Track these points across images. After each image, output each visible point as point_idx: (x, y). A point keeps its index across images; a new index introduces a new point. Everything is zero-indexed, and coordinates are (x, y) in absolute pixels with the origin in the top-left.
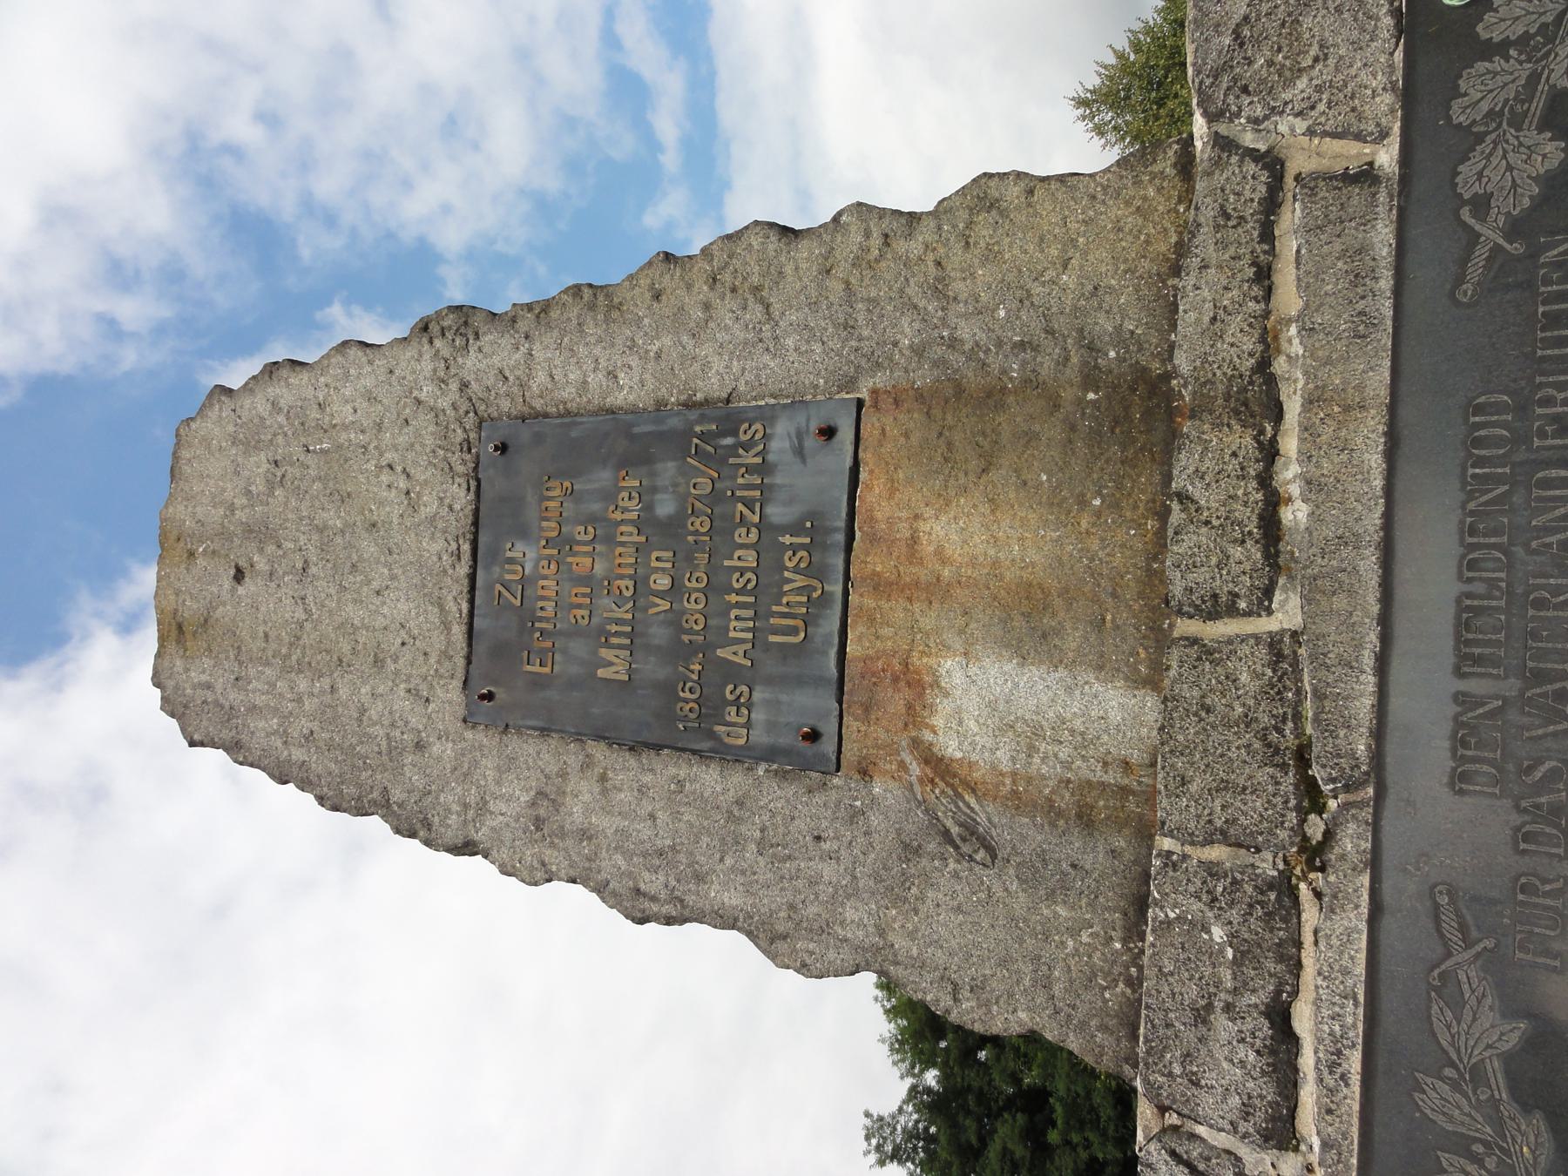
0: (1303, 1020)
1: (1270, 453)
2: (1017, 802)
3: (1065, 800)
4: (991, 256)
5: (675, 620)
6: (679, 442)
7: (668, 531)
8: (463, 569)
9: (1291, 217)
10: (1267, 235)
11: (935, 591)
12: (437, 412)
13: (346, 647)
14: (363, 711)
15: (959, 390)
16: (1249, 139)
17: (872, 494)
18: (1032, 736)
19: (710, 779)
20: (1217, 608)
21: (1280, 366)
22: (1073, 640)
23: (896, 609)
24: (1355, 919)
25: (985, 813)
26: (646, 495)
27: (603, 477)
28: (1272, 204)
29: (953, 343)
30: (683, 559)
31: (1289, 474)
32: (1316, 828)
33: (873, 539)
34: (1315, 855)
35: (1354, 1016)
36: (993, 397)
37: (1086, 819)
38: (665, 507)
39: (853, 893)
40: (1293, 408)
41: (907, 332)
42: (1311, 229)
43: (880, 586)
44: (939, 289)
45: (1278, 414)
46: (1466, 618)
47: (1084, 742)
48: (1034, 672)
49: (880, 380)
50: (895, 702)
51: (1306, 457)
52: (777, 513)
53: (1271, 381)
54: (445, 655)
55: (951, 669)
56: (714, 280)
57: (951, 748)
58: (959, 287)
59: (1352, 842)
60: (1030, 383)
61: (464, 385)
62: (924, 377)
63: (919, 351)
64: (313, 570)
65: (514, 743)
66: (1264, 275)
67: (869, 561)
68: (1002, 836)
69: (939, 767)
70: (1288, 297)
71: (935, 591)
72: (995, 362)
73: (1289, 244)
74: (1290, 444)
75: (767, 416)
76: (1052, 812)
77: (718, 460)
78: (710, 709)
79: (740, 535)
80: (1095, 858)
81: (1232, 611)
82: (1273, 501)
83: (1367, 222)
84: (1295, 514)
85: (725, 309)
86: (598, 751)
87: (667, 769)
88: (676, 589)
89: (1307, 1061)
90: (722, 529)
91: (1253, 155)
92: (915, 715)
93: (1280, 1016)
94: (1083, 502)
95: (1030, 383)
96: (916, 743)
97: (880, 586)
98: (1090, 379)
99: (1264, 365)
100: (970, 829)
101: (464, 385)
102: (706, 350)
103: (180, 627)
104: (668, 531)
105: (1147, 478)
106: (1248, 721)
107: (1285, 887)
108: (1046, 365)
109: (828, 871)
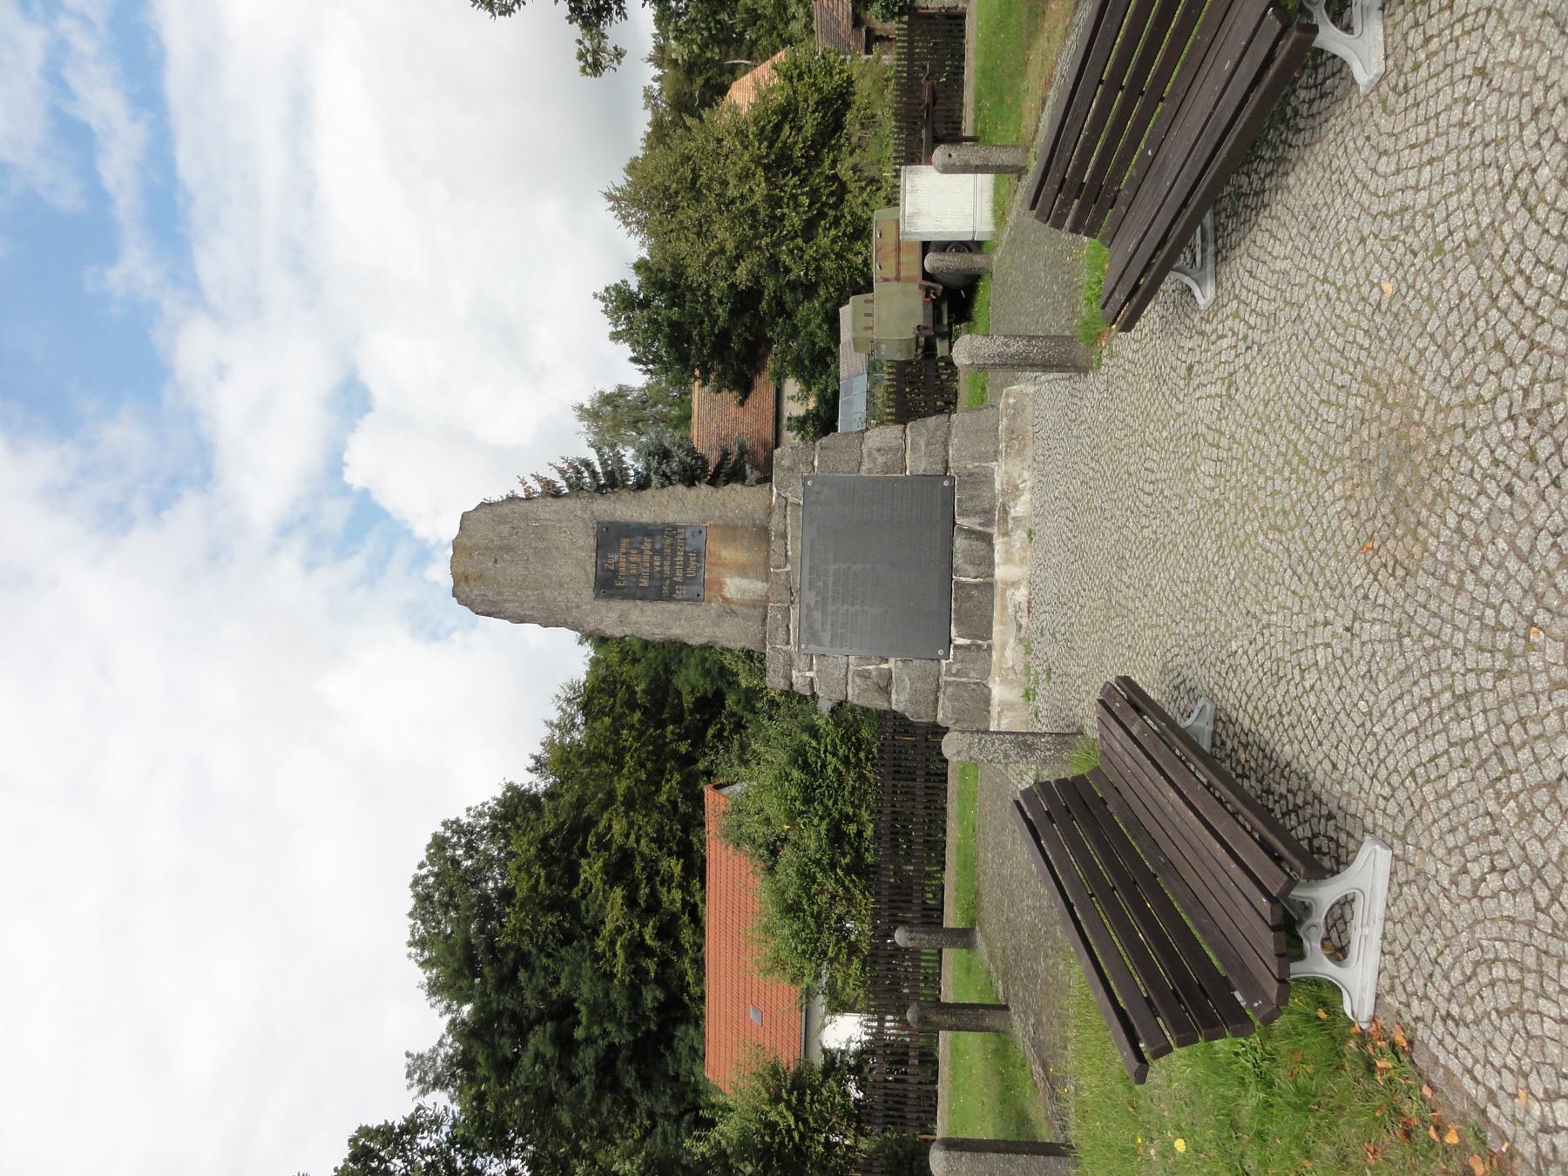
2: (741, 605)
5: (661, 572)
7: (660, 552)
8: (594, 560)
9: (789, 508)
11: (724, 565)
12: (583, 519)
18: (744, 592)
19: (672, 606)
20: (778, 567)
25: (735, 607)
26: (653, 543)
27: (639, 538)
30: (663, 558)
36: (735, 528)
37: (754, 606)
38: (658, 546)
41: (717, 513)
43: (713, 564)
44: (724, 505)
46: (811, 568)
47: (754, 593)
50: (716, 587)
52: (688, 549)
54: (587, 582)
55: (728, 580)
57: (728, 596)
59: (797, 600)
62: (721, 523)
63: (720, 517)
67: (709, 559)
68: (739, 612)
69: (726, 600)
70: (789, 521)
71: (724, 565)
75: (685, 527)
76: (748, 606)
77: (673, 536)
78: (672, 591)
80: (756, 613)
84: (790, 553)
86: (639, 603)
88: (661, 565)
90: (674, 553)
92: (720, 590)
97: (713, 564)
100: (732, 611)
109: (702, 623)
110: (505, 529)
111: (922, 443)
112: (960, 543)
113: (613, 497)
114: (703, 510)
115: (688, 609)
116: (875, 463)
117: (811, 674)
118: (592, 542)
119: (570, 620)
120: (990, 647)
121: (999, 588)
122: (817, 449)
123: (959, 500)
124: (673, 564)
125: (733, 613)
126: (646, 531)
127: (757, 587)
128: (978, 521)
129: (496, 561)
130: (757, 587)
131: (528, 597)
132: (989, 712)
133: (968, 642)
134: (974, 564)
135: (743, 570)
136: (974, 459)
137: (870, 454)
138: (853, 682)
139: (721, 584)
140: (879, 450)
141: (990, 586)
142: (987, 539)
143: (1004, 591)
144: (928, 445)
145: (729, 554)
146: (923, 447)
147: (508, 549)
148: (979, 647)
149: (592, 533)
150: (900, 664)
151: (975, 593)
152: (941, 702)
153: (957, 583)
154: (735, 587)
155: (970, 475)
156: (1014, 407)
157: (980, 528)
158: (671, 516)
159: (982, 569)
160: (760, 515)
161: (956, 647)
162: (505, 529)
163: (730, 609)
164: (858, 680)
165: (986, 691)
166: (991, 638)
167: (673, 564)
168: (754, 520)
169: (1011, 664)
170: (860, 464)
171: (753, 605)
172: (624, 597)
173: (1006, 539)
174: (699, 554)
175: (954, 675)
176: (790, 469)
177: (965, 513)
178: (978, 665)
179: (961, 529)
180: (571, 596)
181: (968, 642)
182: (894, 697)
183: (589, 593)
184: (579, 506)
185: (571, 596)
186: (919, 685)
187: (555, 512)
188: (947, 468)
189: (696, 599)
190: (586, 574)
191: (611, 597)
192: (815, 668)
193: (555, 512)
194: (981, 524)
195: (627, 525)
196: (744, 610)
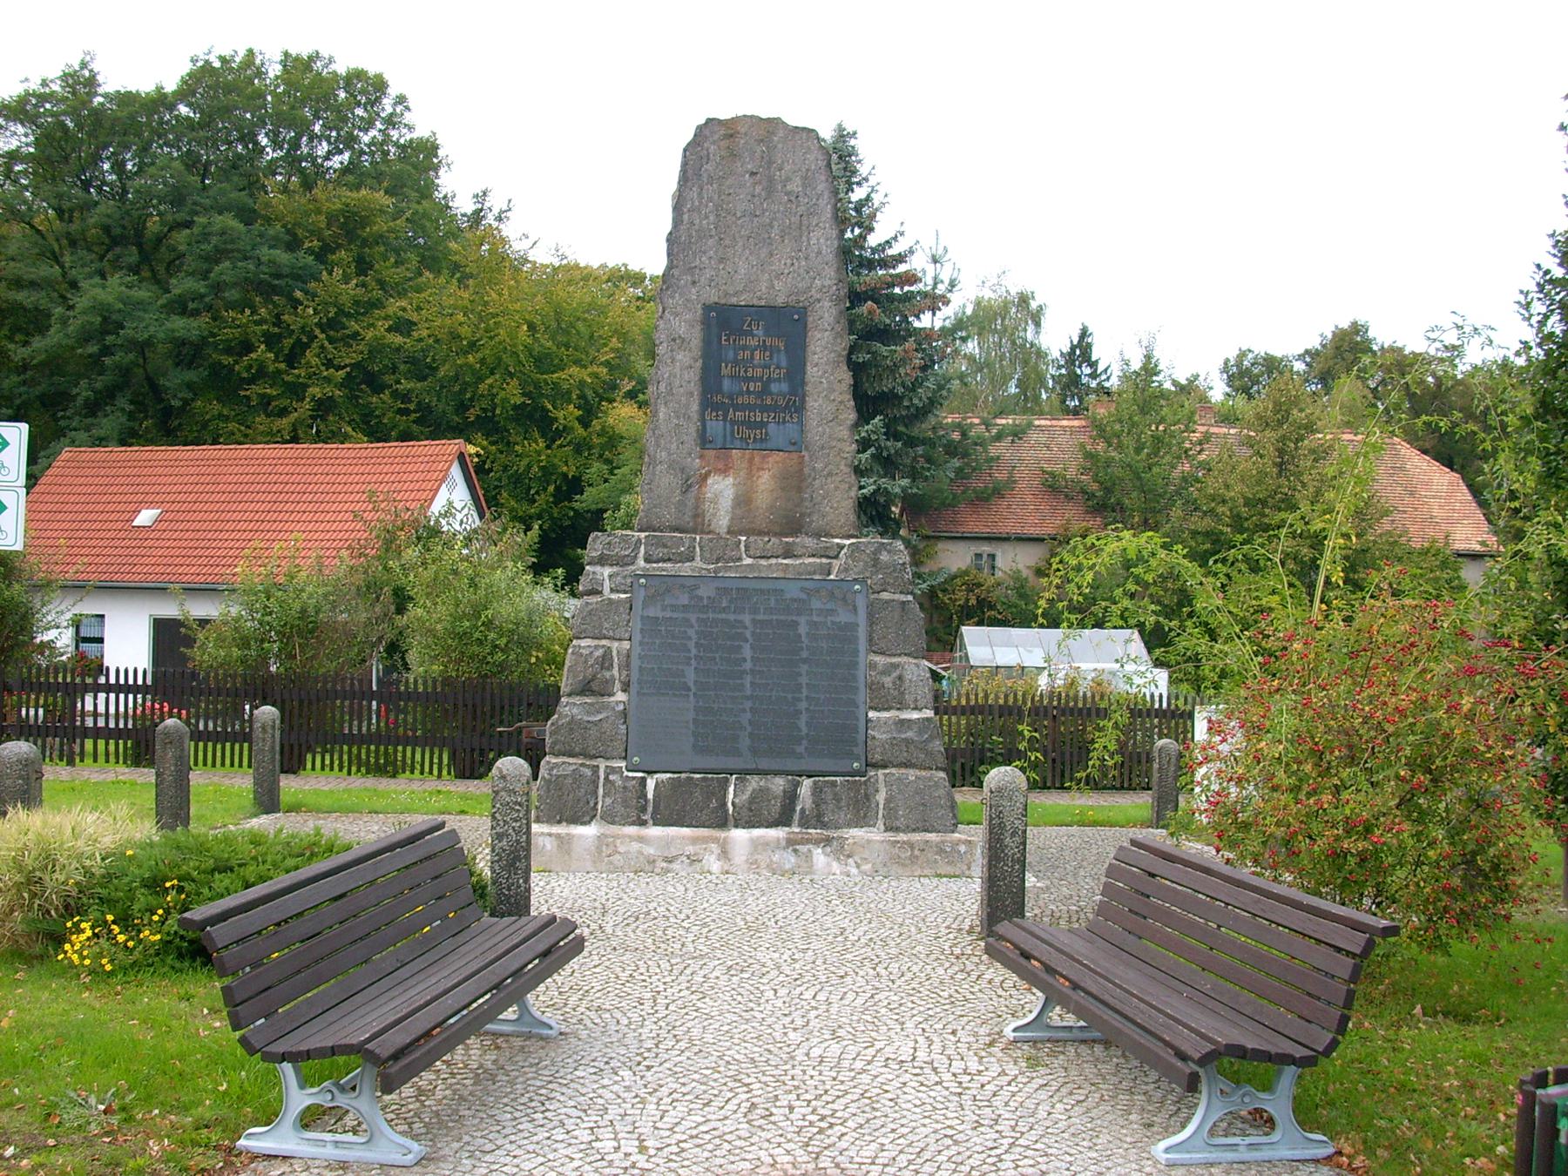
1: (777, 557)
2: (698, 499)
3: (700, 511)
4: (837, 488)
6: (793, 392)
8: (756, 302)
9: (824, 560)
10: (822, 556)
11: (750, 475)
12: (809, 288)
13: (727, 242)
14: (704, 253)
15: (802, 481)
17: (777, 457)
18: (715, 501)
19: (695, 407)
22: (738, 512)
23: (745, 465)
28: (828, 557)
29: (814, 479)
33: (764, 457)
36: (800, 490)
37: (696, 516)
39: (669, 454)
41: (819, 466)
42: (821, 564)
43: (751, 461)
44: (830, 474)
46: (746, 590)
48: (730, 503)
49: (807, 458)
50: (721, 466)
54: (726, 294)
56: (841, 402)
57: (710, 481)
58: (829, 480)
60: (802, 500)
61: (819, 301)
62: (806, 470)
64: (756, 220)
65: (698, 328)
66: (813, 556)
69: (705, 477)
71: (750, 475)
72: (808, 490)
75: (801, 423)
76: (697, 507)
78: (716, 407)
79: (765, 415)
80: (687, 518)
85: (832, 407)
86: (699, 364)
87: (695, 388)
90: (765, 409)
95: (802, 500)
96: (710, 472)
97: (751, 461)
98: (802, 515)
100: (690, 486)
101: (819, 301)
102: (821, 401)
103: (731, 136)
104: (765, 391)
105: (777, 529)
108: (807, 504)
109: (674, 446)
110: (795, 186)
111: (910, 734)
112: (779, 784)
113: (838, 328)
114: (823, 448)
115: (692, 429)
116: (883, 673)
117: (606, 590)
118: (780, 300)
119: (676, 272)
120: (643, 823)
121: (721, 834)
122: (903, 598)
123: (834, 784)
124: (751, 408)
125: (686, 488)
126: (796, 374)
127: (722, 520)
128: (807, 806)
129: (753, 174)
130: (722, 520)
131: (707, 217)
132: (559, 822)
133: (650, 796)
134: (750, 803)
135: (743, 501)
136: (888, 801)
137: (895, 666)
138: (596, 647)
139: (724, 471)
140: (900, 678)
141: (722, 822)
142: (783, 820)
143: (716, 840)
144: (907, 742)
145: (765, 481)
146: (903, 736)
147: (770, 190)
148: (644, 809)
149: (792, 300)
150: (621, 707)
151: (714, 804)
152: (571, 760)
153: (727, 780)
154: (722, 490)
155: (867, 797)
156: (954, 850)
157: (798, 808)
158: (816, 405)
159: (745, 812)
160: (817, 522)
161: (643, 780)
162: (795, 186)
163: (692, 484)
164: (600, 652)
165: (587, 818)
166: (655, 824)
167: (751, 408)
168: (810, 515)
169: (622, 849)
170: (883, 653)
171: (698, 515)
172: (707, 342)
173: (784, 843)
174: (764, 445)
175: (606, 778)
176: (876, 562)
177: (817, 790)
178: (620, 809)
179: (797, 785)
180: (708, 273)
181: (650, 796)
182: (577, 700)
183: (713, 296)
184: (828, 282)
185: (708, 273)
186: (593, 732)
187: (819, 253)
188: (876, 766)
189: (704, 441)
190: (736, 293)
191: (706, 322)
192: (614, 596)
193: (819, 253)
194: (803, 810)
195: (803, 347)
196: (690, 503)
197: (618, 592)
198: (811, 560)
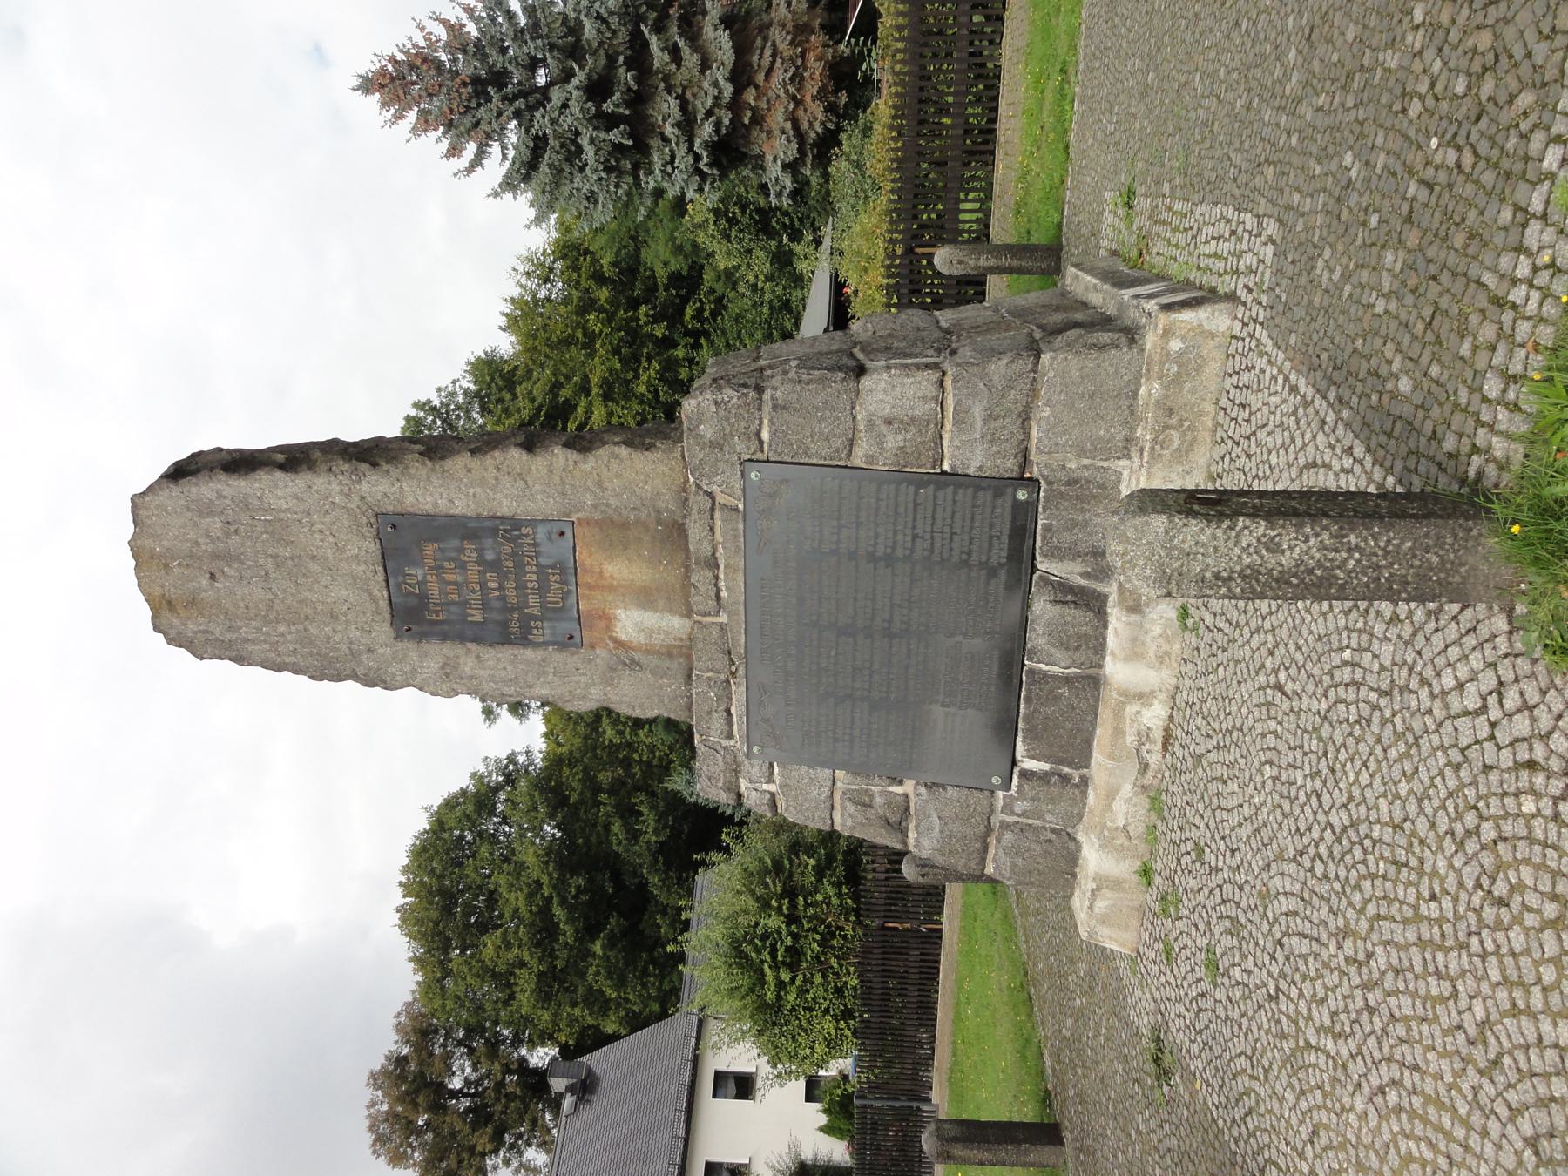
0: (733, 711)
1: (717, 578)
2: (649, 650)
3: (663, 650)
4: (618, 475)
5: (503, 598)
6: (494, 532)
7: (495, 566)
8: (380, 577)
9: (718, 515)
10: (712, 518)
11: (611, 588)
13: (309, 611)
14: (329, 638)
15: (612, 522)
16: (705, 488)
17: (582, 554)
18: (650, 632)
19: (528, 653)
20: (705, 614)
21: (718, 555)
22: (661, 603)
23: (598, 595)
24: (743, 689)
25: (636, 656)
26: (480, 551)
27: (455, 543)
28: (712, 509)
29: (608, 505)
30: (503, 576)
31: (722, 584)
32: (733, 668)
33: (585, 571)
34: (734, 674)
35: (744, 709)
36: (625, 525)
37: (670, 655)
38: (490, 556)
39: (594, 684)
40: (722, 567)
42: (723, 520)
43: (590, 587)
44: (599, 484)
45: (717, 567)
47: (668, 634)
48: (649, 614)
49: (580, 515)
51: (726, 581)
52: (543, 561)
53: (716, 558)
54: (377, 612)
55: (621, 614)
56: (498, 469)
57: (624, 638)
58: (606, 484)
59: (742, 672)
60: (637, 521)
61: (363, 498)
62: (598, 516)
63: (595, 506)
64: (272, 575)
65: (425, 646)
66: (712, 529)
67: (584, 578)
68: (644, 661)
69: (619, 644)
70: (719, 536)
71: (611, 588)
72: (625, 514)
73: (718, 523)
74: (722, 576)
75: (533, 523)
77: (514, 540)
79: (528, 569)
80: (674, 665)
81: (710, 615)
82: (718, 591)
83: (737, 522)
84: (724, 594)
85: (506, 481)
86: (473, 646)
87: (508, 652)
88: (501, 588)
89: (735, 719)
90: (520, 567)
91: (706, 492)
92: (609, 628)
93: (728, 711)
94: (660, 562)
95: (637, 521)
96: (611, 638)
97: (590, 587)
98: (659, 522)
99: (713, 554)
100: (633, 661)
101: (363, 498)
102: (499, 496)
103: (169, 603)
104: (495, 566)
105: (680, 556)
106: (716, 643)
107: (728, 682)
108: (643, 516)
109: (582, 679)
110: (216, 525)
111: (978, 411)
112: (1042, 608)
113: (395, 472)
114: (564, 494)
115: (557, 658)
116: (881, 445)
117: (772, 788)
118: (373, 548)
119: (361, 671)
120: (1084, 781)
121: (1109, 696)
122: (767, 408)
123: (1047, 528)
124: (520, 586)
125: (634, 664)
126: (467, 529)
127: (674, 625)
128: (1079, 568)
129: (212, 576)
130: (674, 625)
131: (282, 635)
132: (1074, 876)
133: (1045, 766)
134: (1067, 649)
135: (645, 597)
136: (1081, 452)
137: (871, 425)
138: (844, 808)
139: (609, 620)
140: (889, 422)
141: (1092, 682)
142: (1094, 604)
143: (1120, 707)
144: (990, 417)
145: (617, 569)
146: (979, 423)
147: (229, 557)
148: (1065, 779)
149: (369, 533)
150: (922, 790)
151: (1064, 691)
152: (992, 851)
153: (1032, 672)
154: (631, 623)
155: (1072, 482)
156: (1180, 358)
157: (1083, 582)
158: (506, 505)
159: (1080, 656)
160: (668, 502)
161: (1026, 775)
162: (216, 525)
163: (627, 658)
164: (851, 808)
165: (1072, 845)
166: (1087, 767)
167: (520, 586)
168: (658, 512)
169: (1121, 822)
170: (852, 442)
171: (668, 653)
172: (445, 637)
173: (1134, 618)
174: (567, 570)
175: (1018, 815)
176: (714, 445)
177: (1056, 554)
178: (1062, 807)
179: (1046, 581)
180: (354, 634)
181: (1045, 766)
182: (912, 835)
183: (383, 630)
184: (335, 487)
185: (354, 634)
186: (955, 828)
187: (295, 497)
188: (1025, 462)
189: (568, 642)
190: (374, 600)
191: (421, 637)
192: (777, 778)
193: (295, 497)
194: (1085, 575)
195: (429, 517)
196: (654, 661)
197: (772, 773)
198: (718, 531)
